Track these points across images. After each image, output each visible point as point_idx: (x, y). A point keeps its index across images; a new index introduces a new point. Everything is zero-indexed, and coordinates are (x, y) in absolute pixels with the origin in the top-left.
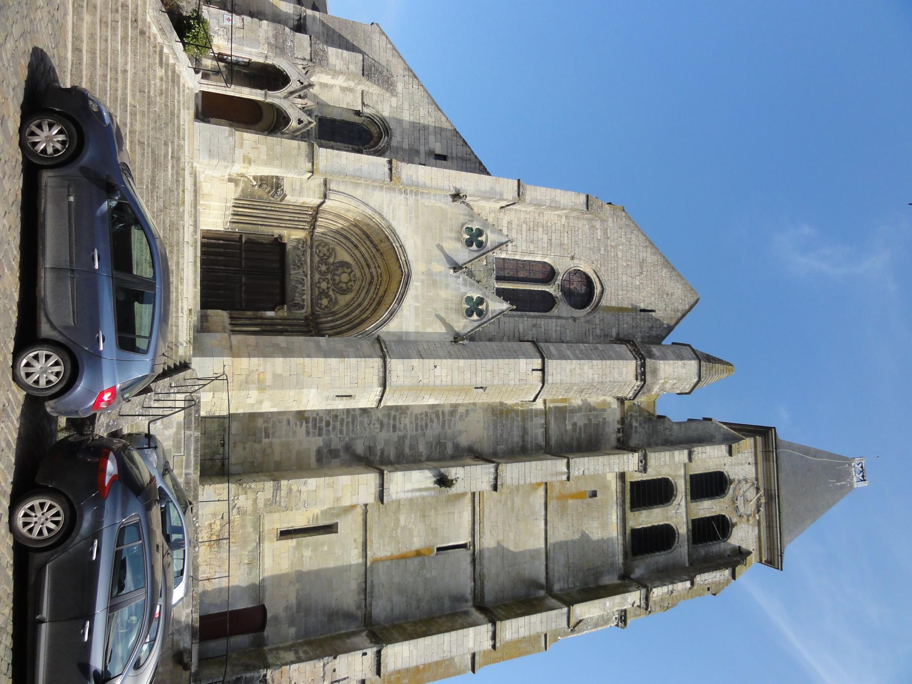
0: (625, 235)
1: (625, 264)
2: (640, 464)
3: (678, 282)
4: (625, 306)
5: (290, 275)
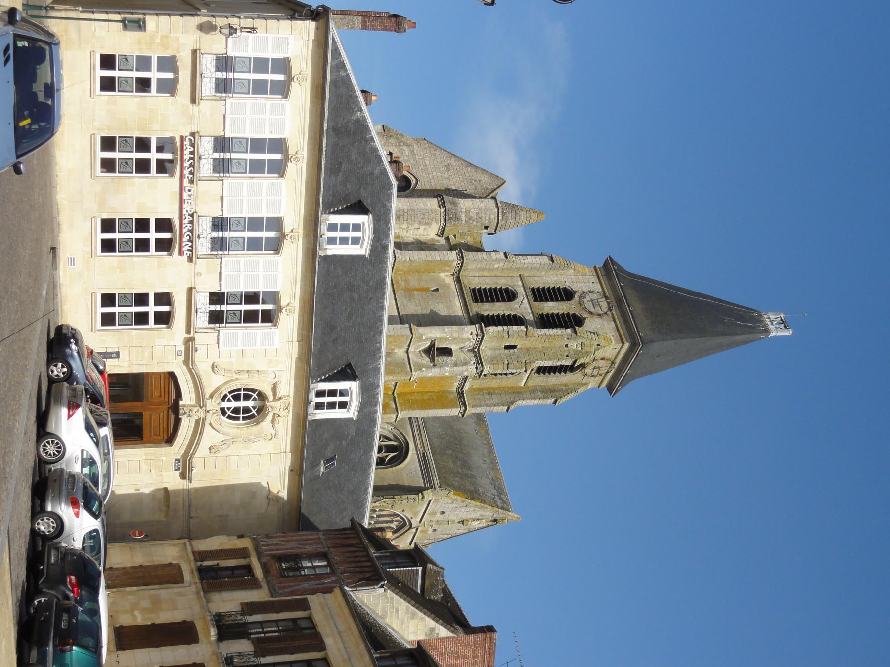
0: (430, 152)
1: (433, 167)
2: (458, 257)
3: (483, 174)
4: (437, 188)
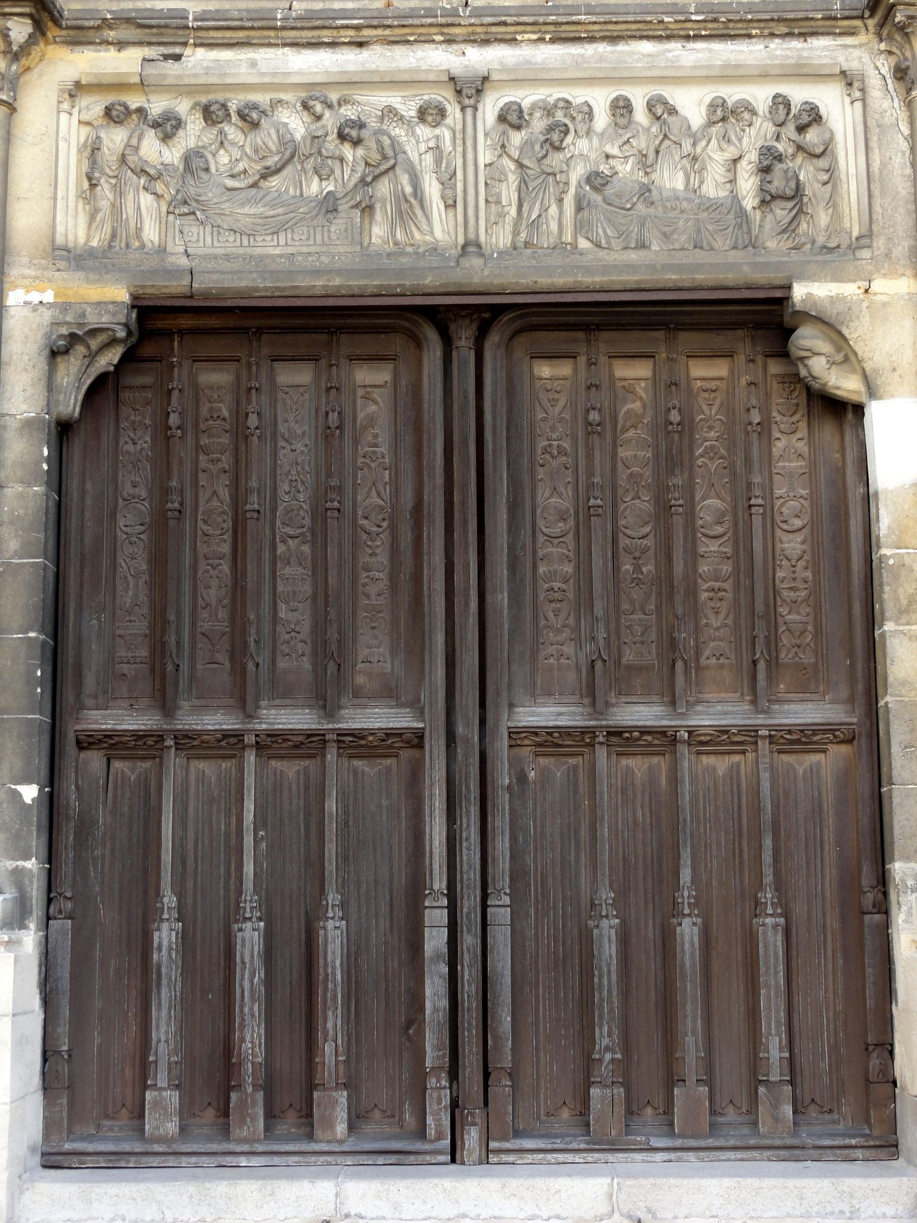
5: (471, 247)
